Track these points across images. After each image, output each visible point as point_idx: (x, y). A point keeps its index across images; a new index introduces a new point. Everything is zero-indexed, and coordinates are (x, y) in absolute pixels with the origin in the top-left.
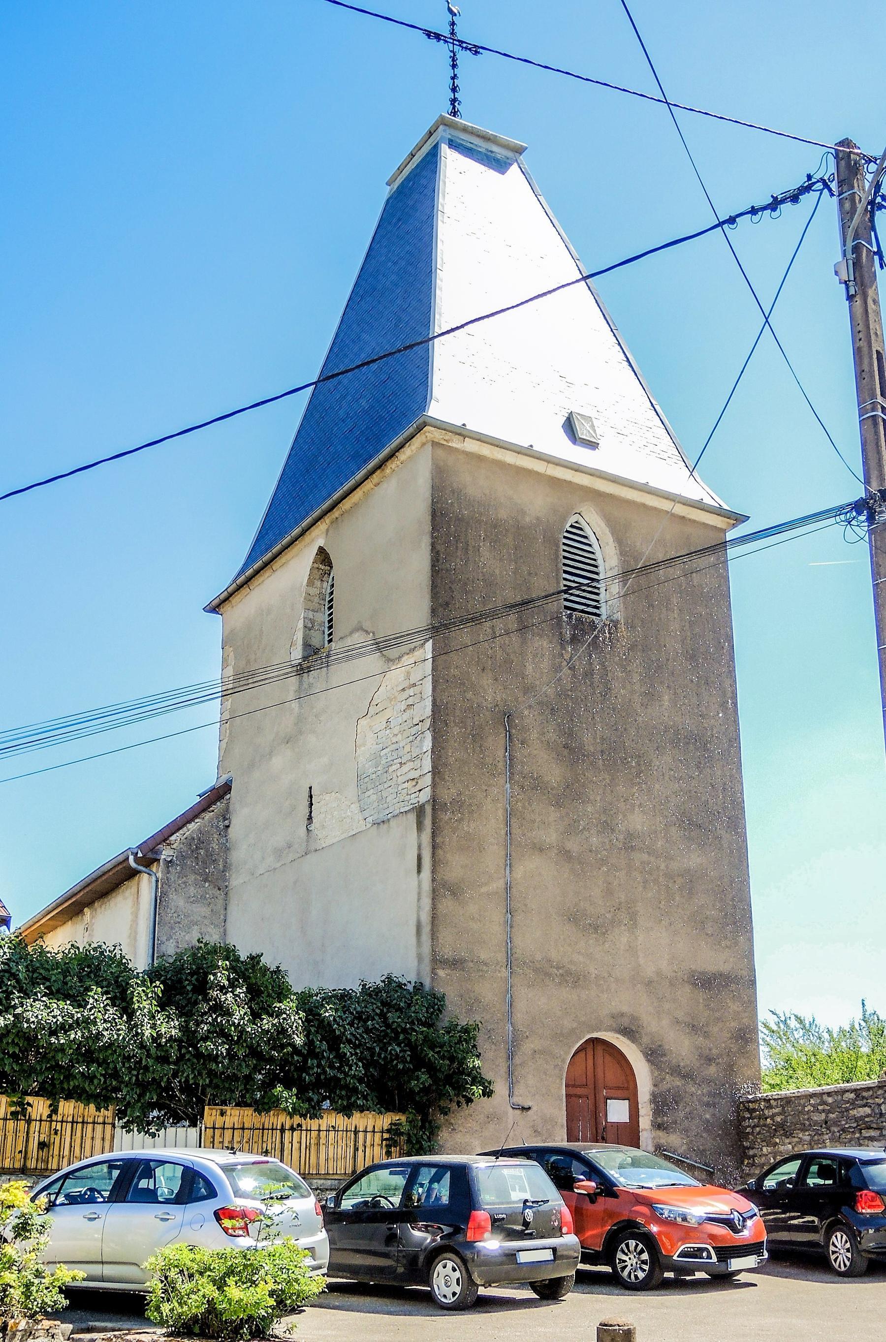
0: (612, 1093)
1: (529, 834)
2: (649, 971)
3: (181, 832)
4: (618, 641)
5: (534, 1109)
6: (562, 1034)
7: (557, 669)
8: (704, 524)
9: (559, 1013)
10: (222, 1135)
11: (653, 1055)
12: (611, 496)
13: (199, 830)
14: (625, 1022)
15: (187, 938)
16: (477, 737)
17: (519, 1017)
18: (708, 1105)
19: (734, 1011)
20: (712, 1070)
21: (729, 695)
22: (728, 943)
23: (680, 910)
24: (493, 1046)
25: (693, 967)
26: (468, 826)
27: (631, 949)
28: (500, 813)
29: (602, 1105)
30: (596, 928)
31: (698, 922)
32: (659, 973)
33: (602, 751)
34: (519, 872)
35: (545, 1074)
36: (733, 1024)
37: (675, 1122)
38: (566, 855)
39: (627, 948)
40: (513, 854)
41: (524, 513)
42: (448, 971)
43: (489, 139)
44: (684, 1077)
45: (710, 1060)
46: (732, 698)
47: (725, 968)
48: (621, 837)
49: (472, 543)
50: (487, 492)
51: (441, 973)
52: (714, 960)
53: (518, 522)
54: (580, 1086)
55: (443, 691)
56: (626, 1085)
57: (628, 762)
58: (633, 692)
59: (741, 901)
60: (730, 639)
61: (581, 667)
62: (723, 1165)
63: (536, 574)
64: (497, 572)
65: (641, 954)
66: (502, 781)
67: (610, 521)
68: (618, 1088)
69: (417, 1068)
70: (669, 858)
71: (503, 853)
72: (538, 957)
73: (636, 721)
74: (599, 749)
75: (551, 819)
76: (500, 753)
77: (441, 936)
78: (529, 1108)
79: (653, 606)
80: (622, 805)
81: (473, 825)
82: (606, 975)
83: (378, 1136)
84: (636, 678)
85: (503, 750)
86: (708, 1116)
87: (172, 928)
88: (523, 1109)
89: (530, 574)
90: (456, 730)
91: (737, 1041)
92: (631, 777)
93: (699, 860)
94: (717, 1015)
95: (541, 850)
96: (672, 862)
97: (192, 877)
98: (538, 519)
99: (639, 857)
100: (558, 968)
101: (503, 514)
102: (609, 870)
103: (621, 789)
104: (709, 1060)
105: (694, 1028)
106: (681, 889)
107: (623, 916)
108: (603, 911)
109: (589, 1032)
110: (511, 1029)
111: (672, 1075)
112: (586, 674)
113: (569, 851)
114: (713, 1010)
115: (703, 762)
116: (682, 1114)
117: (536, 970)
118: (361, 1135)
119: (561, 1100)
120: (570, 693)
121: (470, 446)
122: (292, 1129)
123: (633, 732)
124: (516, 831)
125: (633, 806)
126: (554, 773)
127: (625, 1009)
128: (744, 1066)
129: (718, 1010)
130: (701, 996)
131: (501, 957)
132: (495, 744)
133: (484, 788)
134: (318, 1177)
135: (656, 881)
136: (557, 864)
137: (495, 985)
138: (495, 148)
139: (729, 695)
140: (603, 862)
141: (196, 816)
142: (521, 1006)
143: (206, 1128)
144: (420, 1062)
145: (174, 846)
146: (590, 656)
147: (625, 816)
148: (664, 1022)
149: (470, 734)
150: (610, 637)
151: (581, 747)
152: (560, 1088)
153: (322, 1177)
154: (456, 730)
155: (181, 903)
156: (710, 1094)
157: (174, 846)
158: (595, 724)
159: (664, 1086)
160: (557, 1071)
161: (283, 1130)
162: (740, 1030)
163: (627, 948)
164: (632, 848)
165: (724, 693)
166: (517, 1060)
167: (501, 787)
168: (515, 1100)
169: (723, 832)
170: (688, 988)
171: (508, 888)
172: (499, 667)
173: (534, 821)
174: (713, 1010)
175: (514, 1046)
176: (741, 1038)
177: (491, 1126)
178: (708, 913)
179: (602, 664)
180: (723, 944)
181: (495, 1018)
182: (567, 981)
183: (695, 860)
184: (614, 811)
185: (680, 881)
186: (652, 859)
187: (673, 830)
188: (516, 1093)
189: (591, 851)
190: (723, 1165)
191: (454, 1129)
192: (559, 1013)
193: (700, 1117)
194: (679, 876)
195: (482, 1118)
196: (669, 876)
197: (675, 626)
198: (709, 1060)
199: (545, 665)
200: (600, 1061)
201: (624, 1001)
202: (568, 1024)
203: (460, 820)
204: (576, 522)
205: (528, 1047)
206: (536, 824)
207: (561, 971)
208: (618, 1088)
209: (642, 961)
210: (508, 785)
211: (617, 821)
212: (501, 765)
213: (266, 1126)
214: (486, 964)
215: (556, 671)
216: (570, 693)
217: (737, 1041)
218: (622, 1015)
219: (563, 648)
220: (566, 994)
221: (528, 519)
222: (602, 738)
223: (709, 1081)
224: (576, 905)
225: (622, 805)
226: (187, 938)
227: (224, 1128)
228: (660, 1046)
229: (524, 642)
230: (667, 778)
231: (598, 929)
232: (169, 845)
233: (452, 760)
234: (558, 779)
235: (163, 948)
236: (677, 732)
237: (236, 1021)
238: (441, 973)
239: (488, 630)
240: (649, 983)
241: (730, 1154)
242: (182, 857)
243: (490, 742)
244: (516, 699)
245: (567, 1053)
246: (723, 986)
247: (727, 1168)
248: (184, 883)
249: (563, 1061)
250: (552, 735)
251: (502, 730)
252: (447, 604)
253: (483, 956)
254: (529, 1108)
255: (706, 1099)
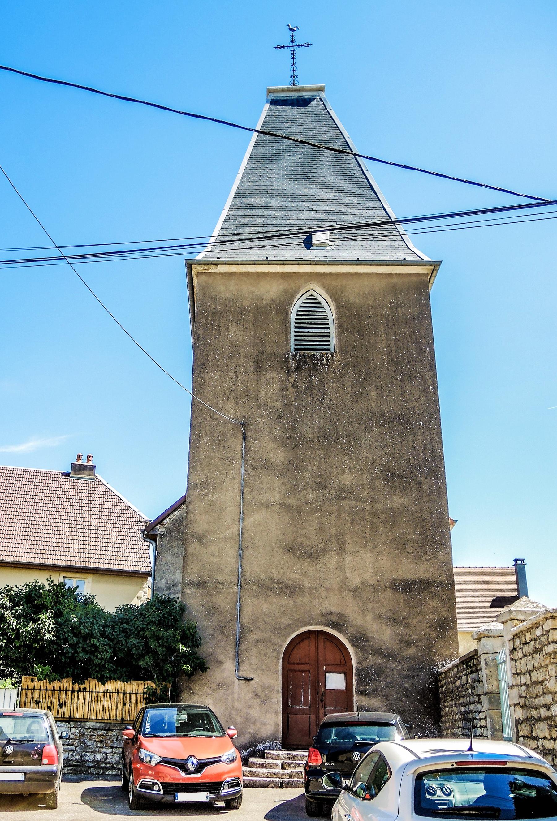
0: (331, 668)
1: (258, 498)
2: (356, 581)
3: (170, 517)
4: (334, 363)
5: (256, 679)
6: (280, 628)
7: (283, 389)
8: (408, 274)
9: (277, 614)
10: (33, 694)
11: (359, 640)
12: (331, 274)
13: (180, 515)
14: (334, 618)
15: (172, 578)
16: (221, 441)
17: (246, 618)
18: (407, 677)
19: (434, 607)
20: (412, 651)
21: (430, 383)
22: (428, 558)
23: (383, 537)
24: (225, 638)
25: (395, 577)
26: (213, 497)
27: (340, 567)
28: (237, 486)
29: (321, 677)
30: (310, 555)
31: (400, 544)
32: (364, 583)
33: (318, 437)
34: (249, 521)
35: (265, 656)
36: (432, 617)
37: (377, 690)
38: (287, 508)
39: (337, 566)
40: (246, 511)
41: (262, 299)
42: (193, 590)
43: (300, 90)
44: (385, 656)
45: (409, 644)
46: (432, 385)
47: (423, 575)
48: (333, 491)
49: (223, 325)
50: (235, 293)
51: (188, 591)
52: (411, 569)
53: (258, 305)
54: (304, 664)
55: (198, 416)
56: (343, 663)
57: (340, 441)
58: (345, 394)
59: (440, 525)
60: (431, 345)
61: (302, 385)
62: (421, 722)
63: (270, 334)
64: (241, 338)
65: (348, 571)
66: (239, 466)
67: (327, 289)
68: (336, 665)
69: (147, 653)
70: (374, 501)
71: (238, 511)
72: (263, 577)
73: (347, 412)
74: (316, 435)
75: (276, 485)
76: (238, 448)
77: (189, 568)
78: (252, 679)
79: (363, 336)
80: (334, 470)
81: (215, 496)
82: (318, 586)
83: (140, 697)
84: (348, 385)
85: (240, 447)
86: (407, 685)
87: (164, 573)
88: (246, 679)
89: (265, 335)
90: (206, 439)
91: (436, 629)
92: (342, 450)
93: (401, 501)
94: (417, 610)
95: (267, 507)
96: (377, 504)
97: (176, 543)
98: (273, 300)
99: (347, 504)
100: (278, 584)
101: (247, 303)
102: (322, 515)
103: (333, 459)
104: (409, 644)
105: (395, 621)
106: (384, 522)
107: (334, 545)
108: (317, 543)
109: (302, 627)
110: (239, 626)
111: (374, 655)
112: (306, 389)
113: (290, 505)
114: (413, 607)
115: (405, 432)
116: (382, 684)
117: (261, 586)
118: (128, 695)
119: (278, 674)
120: (293, 403)
121: (223, 269)
122: (79, 691)
123: (344, 421)
124: (248, 495)
125: (343, 470)
126: (278, 456)
127: (333, 609)
128: (442, 648)
129: (417, 607)
130: (402, 598)
131: (234, 579)
132: (235, 444)
133: (225, 472)
134: (97, 721)
135: (363, 519)
136: (279, 514)
137: (228, 597)
138: (304, 94)
139: (430, 383)
140: (317, 510)
141: (178, 507)
142: (247, 611)
143: (22, 689)
144: (147, 649)
145: (166, 526)
146: (311, 377)
147: (336, 477)
148: (368, 617)
149: (217, 440)
150: (327, 363)
151: (302, 435)
152: (277, 665)
153: (100, 721)
154: (206, 439)
155: (169, 558)
156: (409, 669)
157: (166, 526)
158: (313, 420)
159: (368, 663)
160: (275, 654)
161: (73, 691)
162: (439, 620)
163: (337, 566)
164: (342, 498)
165: (426, 382)
166: (243, 647)
167: (238, 471)
168: (241, 673)
169: (424, 479)
170: (389, 592)
171: (241, 533)
172: (240, 395)
173: (262, 489)
174: (413, 607)
175: (241, 638)
176: (440, 626)
177: (221, 692)
178: (409, 537)
179: (321, 381)
180: (423, 558)
181: (228, 619)
182: (285, 593)
183: (398, 500)
184: (328, 474)
185: (383, 517)
186: (359, 504)
187: (378, 483)
188: (241, 668)
189: (307, 503)
190: (421, 722)
191: (193, 693)
192: (277, 614)
193: (400, 686)
194: (382, 513)
195: (214, 686)
196: (374, 514)
197: (382, 346)
198: (409, 644)
199: (275, 388)
200: (321, 646)
201: (332, 604)
202: (285, 621)
203: (206, 494)
204: (312, 295)
205: (252, 637)
206: (264, 491)
207: (280, 586)
208: (336, 665)
209: (348, 575)
210: (243, 468)
211: (330, 481)
212: (238, 456)
213: (62, 689)
214: (222, 584)
215: (283, 391)
216: (293, 403)
217: (436, 629)
218: (331, 613)
219: (289, 375)
220: (284, 601)
221: (265, 302)
222: (319, 428)
223: (409, 659)
224: (294, 540)
225: (334, 470)
226: (172, 578)
227: (34, 689)
228: (365, 635)
229: (259, 376)
230: (373, 447)
231: (312, 555)
232: (163, 525)
233: (202, 457)
234: (283, 459)
235: (158, 584)
236: (383, 415)
237: (14, 627)
238: (188, 591)
239: (233, 374)
240: (356, 590)
241: (428, 714)
242: (170, 531)
243: (230, 443)
244: (252, 413)
245: (284, 641)
246: (423, 589)
247: (425, 724)
248: (172, 546)
249: (281, 646)
250: (278, 431)
251: (240, 434)
252: (204, 364)
253: (220, 579)
254: (252, 679)
255: (405, 673)
